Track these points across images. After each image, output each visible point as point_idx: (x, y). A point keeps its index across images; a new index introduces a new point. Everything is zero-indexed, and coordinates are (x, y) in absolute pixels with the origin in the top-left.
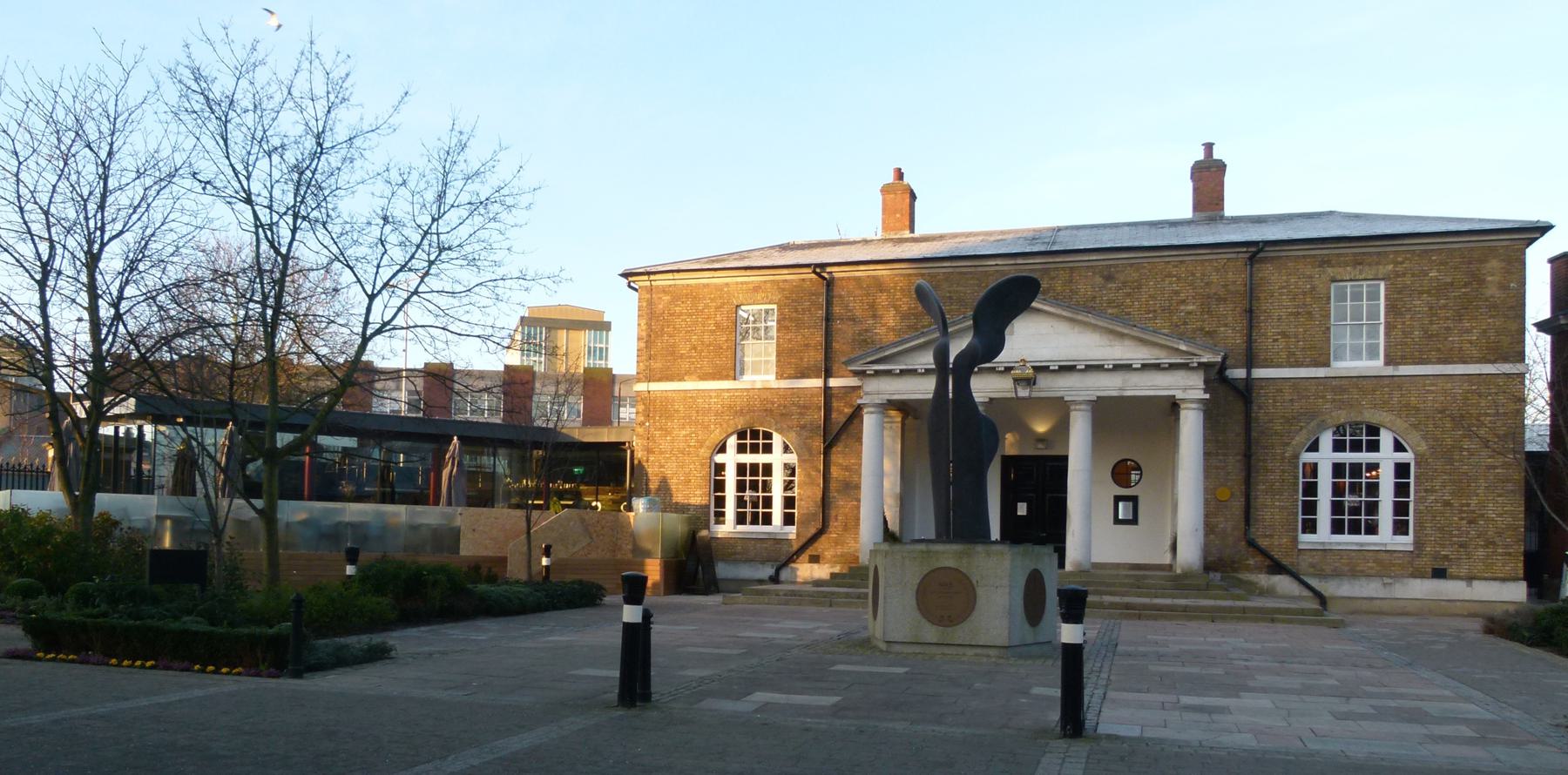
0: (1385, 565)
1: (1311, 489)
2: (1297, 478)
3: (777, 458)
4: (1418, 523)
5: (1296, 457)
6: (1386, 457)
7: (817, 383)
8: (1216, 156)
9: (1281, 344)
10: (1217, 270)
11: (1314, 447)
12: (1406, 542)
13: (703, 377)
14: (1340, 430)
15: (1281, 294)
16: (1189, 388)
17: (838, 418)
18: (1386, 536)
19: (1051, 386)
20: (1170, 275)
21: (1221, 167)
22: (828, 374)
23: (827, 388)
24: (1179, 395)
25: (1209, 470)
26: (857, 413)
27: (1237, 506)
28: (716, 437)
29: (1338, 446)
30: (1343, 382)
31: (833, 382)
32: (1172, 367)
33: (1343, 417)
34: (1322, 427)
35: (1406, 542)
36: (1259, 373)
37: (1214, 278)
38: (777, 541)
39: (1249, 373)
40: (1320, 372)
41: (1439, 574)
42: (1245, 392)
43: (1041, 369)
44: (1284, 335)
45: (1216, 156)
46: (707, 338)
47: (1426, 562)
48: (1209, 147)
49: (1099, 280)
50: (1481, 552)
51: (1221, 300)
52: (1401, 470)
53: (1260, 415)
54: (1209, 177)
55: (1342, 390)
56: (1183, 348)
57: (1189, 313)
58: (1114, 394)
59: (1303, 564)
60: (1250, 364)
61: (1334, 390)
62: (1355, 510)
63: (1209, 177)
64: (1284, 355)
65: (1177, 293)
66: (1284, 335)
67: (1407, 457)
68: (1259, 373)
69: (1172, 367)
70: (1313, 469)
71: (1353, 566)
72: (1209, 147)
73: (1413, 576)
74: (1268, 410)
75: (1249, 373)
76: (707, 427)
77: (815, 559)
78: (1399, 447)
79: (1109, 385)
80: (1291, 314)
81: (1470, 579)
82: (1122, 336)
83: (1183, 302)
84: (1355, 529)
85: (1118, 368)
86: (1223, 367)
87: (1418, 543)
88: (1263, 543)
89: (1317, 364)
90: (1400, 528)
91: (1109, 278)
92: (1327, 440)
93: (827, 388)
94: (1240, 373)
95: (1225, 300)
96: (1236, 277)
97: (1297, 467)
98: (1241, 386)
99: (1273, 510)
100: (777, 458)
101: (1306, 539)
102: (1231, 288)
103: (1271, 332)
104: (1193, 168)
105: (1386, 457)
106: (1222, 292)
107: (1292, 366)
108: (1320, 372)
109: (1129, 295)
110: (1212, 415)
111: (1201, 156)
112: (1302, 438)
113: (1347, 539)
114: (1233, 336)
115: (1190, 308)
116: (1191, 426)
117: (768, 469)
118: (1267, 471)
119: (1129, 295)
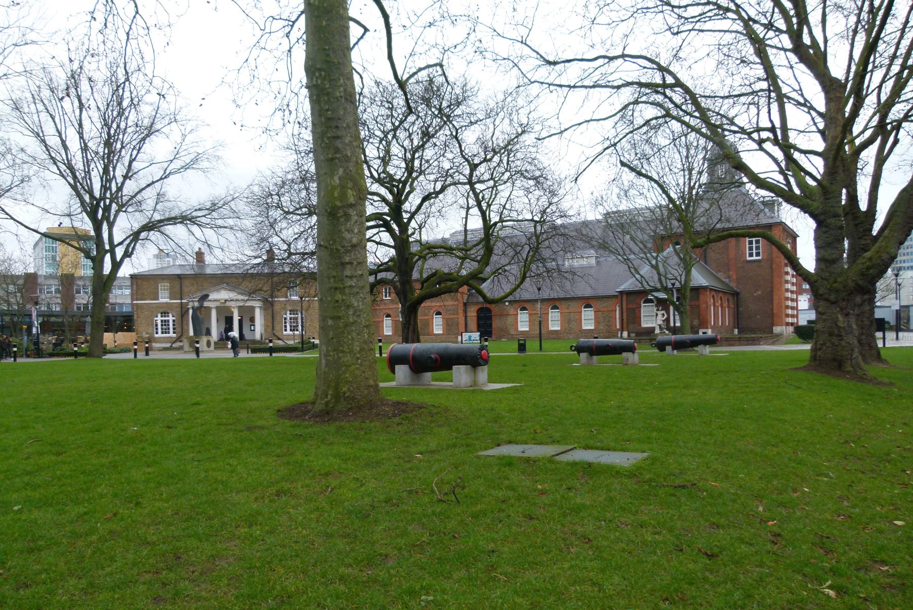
22: (181, 299)
38: (171, 338)
43: (226, 301)
59: (284, 338)
70: (285, 319)
99: (277, 327)
100: (171, 318)
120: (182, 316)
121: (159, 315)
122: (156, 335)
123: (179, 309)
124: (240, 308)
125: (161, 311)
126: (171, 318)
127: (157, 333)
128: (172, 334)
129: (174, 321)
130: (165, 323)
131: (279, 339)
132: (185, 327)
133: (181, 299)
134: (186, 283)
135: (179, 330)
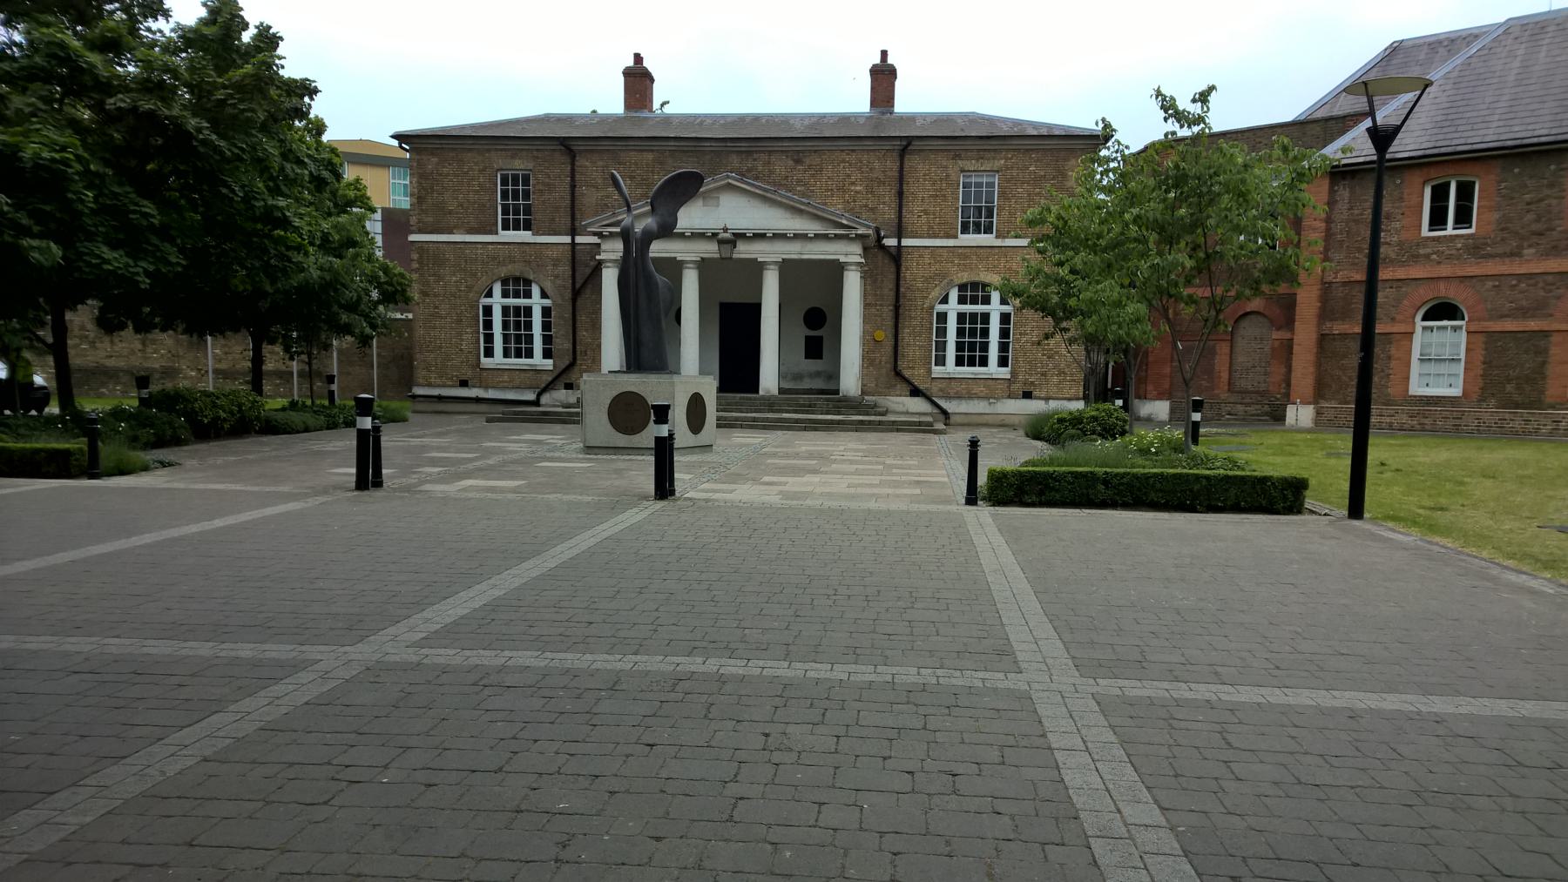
0: (991, 389)
3: (536, 302)
4: (1015, 359)
5: (932, 308)
6: (995, 308)
7: (567, 239)
8: (890, 61)
9: (924, 219)
11: (945, 300)
13: (471, 231)
14: (962, 287)
16: (850, 253)
17: (583, 272)
18: (993, 369)
19: (744, 250)
21: (892, 72)
22: (573, 232)
23: (573, 244)
24: (842, 259)
25: (866, 319)
26: (598, 268)
27: (889, 344)
28: (484, 282)
29: (962, 300)
31: (579, 239)
32: (837, 237)
33: (965, 277)
34: (951, 285)
35: (1004, 372)
36: (906, 242)
40: (951, 242)
41: (1027, 395)
42: (896, 256)
44: (926, 212)
45: (890, 61)
47: (1018, 387)
48: (884, 54)
49: (791, 163)
50: (1055, 379)
51: (881, 183)
53: (907, 274)
54: (883, 76)
59: (934, 389)
62: (972, 347)
63: (883, 76)
66: (926, 212)
68: (906, 242)
69: (837, 237)
71: (965, 390)
72: (884, 54)
73: (1009, 397)
74: (913, 271)
76: (475, 275)
77: (569, 386)
79: (793, 251)
81: (1047, 399)
82: (800, 212)
84: (972, 363)
85: (797, 237)
86: (879, 239)
87: (1013, 373)
89: (948, 236)
91: (798, 161)
92: (954, 295)
93: (573, 244)
94: (891, 242)
96: (892, 165)
98: (893, 251)
99: (912, 347)
101: (937, 371)
103: (916, 209)
108: (951, 242)
110: (868, 277)
112: (936, 293)
113: (966, 371)
114: (888, 213)
116: (853, 285)
117: (528, 311)
120: (576, 293)
121: (497, 289)
123: (565, 269)
124: (788, 269)
125: (504, 271)
126: (536, 302)
127: (489, 352)
128: (538, 359)
129: (546, 312)
130: (518, 319)
131: (915, 392)
132: (583, 334)
133: (573, 232)
134: (591, 168)
135: (562, 343)
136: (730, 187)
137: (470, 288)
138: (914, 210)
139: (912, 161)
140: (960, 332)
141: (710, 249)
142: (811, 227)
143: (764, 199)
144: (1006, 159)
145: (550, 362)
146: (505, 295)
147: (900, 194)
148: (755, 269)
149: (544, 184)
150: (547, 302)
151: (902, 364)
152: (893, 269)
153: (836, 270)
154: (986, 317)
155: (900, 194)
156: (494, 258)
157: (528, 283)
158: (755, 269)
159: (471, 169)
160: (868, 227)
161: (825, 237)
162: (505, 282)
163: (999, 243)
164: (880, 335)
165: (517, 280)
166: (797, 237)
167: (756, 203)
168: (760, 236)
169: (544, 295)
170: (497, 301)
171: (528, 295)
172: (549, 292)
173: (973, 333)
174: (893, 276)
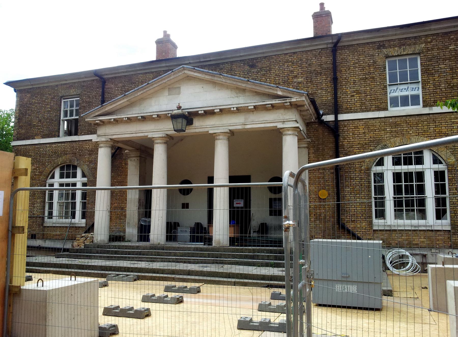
1: (380, 190)
2: (370, 182)
5: (369, 169)
9: (357, 97)
10: (315, 56)
12: (445, 224)
13: (44, 137)
15: (355, 67)
19: (200, 126)
20: (287, 61)
24: (280, 126)
28: (48, 169)
30: (398, 119)
35: (445, 224)
36: (342, 117)
37: (314, 61)
39: (336, 117)
40: (382, 114)
44: (358, 92)
46: (46, 115)
48: (322, 5)
49: (247, 68)
51: (318, 74)
52: (439, 176)
55: (396, 125)
56: (280, 93)
57: (299, 83)
58: (240, 127)
60: (336, 113)
61: (391, 125)
64: (358, 104)
65: (292, 72)
66: (358, 92)
67: (441, 167)
68: (342, 117)
70: (380, 177)
72: (322, 5)
75: (336, 117)
76: (44, 164)
78: (436, 161)
79: (236, 122)
80: (362, 79)
82: (244, 90)
83: (296, 77)
85: (239, 110)
86: (319, 116)
88: (350, 226)
89: (379, 109)
90: (440, 215)
91: (253, 66)
94: (330, 118)
95: (321, 74)
97: (369, 175)
98: (332, 125)
101: (378, 223)
102: (325, 66)
104: (313, 16)
105: (428, 168)
106: (318, 69)
107: (363, 111)
108: (382, 114)
109: (264, 75)
111: (318, 9)
114: (324, 96)
115: (300, 80)
118: (351, 179)
119: (264, 75)
121: (57, 173)
122: (48, 222)
125: (60, 160)
136: (189, 79)
137: (41, 173)
138: (347, 94)
139: (341, 55)
140: (397, 190)
141: (167, 127)
142: (250, 101)
143: (214, 84)
144: (426, 43)
145: (84, 221)
146: (62, 176)
147: (335, 80)
148: (209, 140)
149: (86, 102)
150: (85, 180)
151: (345, 218)
152: (332, 139)
153: (276, 135)
154: (420, 176)
155: (335, 80)
156: (55, 153)
157: (75, 167)
158: (209, 140)
159: (47, 98)
160: (301, 95)
161: (265, 108)
162: (62, 168)
163: (427, 111)
164: (324, 194)
165: (68, 166)
166: (239, 110)
167: (208, 87)
168: (209, 113)
169: (84, 176)
170: (57, 180)
171: (75, 176)
172: (86, 173)
173: (409, 190)
174: (332, 145)
